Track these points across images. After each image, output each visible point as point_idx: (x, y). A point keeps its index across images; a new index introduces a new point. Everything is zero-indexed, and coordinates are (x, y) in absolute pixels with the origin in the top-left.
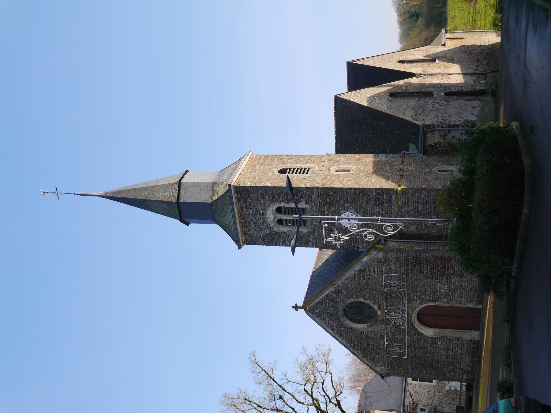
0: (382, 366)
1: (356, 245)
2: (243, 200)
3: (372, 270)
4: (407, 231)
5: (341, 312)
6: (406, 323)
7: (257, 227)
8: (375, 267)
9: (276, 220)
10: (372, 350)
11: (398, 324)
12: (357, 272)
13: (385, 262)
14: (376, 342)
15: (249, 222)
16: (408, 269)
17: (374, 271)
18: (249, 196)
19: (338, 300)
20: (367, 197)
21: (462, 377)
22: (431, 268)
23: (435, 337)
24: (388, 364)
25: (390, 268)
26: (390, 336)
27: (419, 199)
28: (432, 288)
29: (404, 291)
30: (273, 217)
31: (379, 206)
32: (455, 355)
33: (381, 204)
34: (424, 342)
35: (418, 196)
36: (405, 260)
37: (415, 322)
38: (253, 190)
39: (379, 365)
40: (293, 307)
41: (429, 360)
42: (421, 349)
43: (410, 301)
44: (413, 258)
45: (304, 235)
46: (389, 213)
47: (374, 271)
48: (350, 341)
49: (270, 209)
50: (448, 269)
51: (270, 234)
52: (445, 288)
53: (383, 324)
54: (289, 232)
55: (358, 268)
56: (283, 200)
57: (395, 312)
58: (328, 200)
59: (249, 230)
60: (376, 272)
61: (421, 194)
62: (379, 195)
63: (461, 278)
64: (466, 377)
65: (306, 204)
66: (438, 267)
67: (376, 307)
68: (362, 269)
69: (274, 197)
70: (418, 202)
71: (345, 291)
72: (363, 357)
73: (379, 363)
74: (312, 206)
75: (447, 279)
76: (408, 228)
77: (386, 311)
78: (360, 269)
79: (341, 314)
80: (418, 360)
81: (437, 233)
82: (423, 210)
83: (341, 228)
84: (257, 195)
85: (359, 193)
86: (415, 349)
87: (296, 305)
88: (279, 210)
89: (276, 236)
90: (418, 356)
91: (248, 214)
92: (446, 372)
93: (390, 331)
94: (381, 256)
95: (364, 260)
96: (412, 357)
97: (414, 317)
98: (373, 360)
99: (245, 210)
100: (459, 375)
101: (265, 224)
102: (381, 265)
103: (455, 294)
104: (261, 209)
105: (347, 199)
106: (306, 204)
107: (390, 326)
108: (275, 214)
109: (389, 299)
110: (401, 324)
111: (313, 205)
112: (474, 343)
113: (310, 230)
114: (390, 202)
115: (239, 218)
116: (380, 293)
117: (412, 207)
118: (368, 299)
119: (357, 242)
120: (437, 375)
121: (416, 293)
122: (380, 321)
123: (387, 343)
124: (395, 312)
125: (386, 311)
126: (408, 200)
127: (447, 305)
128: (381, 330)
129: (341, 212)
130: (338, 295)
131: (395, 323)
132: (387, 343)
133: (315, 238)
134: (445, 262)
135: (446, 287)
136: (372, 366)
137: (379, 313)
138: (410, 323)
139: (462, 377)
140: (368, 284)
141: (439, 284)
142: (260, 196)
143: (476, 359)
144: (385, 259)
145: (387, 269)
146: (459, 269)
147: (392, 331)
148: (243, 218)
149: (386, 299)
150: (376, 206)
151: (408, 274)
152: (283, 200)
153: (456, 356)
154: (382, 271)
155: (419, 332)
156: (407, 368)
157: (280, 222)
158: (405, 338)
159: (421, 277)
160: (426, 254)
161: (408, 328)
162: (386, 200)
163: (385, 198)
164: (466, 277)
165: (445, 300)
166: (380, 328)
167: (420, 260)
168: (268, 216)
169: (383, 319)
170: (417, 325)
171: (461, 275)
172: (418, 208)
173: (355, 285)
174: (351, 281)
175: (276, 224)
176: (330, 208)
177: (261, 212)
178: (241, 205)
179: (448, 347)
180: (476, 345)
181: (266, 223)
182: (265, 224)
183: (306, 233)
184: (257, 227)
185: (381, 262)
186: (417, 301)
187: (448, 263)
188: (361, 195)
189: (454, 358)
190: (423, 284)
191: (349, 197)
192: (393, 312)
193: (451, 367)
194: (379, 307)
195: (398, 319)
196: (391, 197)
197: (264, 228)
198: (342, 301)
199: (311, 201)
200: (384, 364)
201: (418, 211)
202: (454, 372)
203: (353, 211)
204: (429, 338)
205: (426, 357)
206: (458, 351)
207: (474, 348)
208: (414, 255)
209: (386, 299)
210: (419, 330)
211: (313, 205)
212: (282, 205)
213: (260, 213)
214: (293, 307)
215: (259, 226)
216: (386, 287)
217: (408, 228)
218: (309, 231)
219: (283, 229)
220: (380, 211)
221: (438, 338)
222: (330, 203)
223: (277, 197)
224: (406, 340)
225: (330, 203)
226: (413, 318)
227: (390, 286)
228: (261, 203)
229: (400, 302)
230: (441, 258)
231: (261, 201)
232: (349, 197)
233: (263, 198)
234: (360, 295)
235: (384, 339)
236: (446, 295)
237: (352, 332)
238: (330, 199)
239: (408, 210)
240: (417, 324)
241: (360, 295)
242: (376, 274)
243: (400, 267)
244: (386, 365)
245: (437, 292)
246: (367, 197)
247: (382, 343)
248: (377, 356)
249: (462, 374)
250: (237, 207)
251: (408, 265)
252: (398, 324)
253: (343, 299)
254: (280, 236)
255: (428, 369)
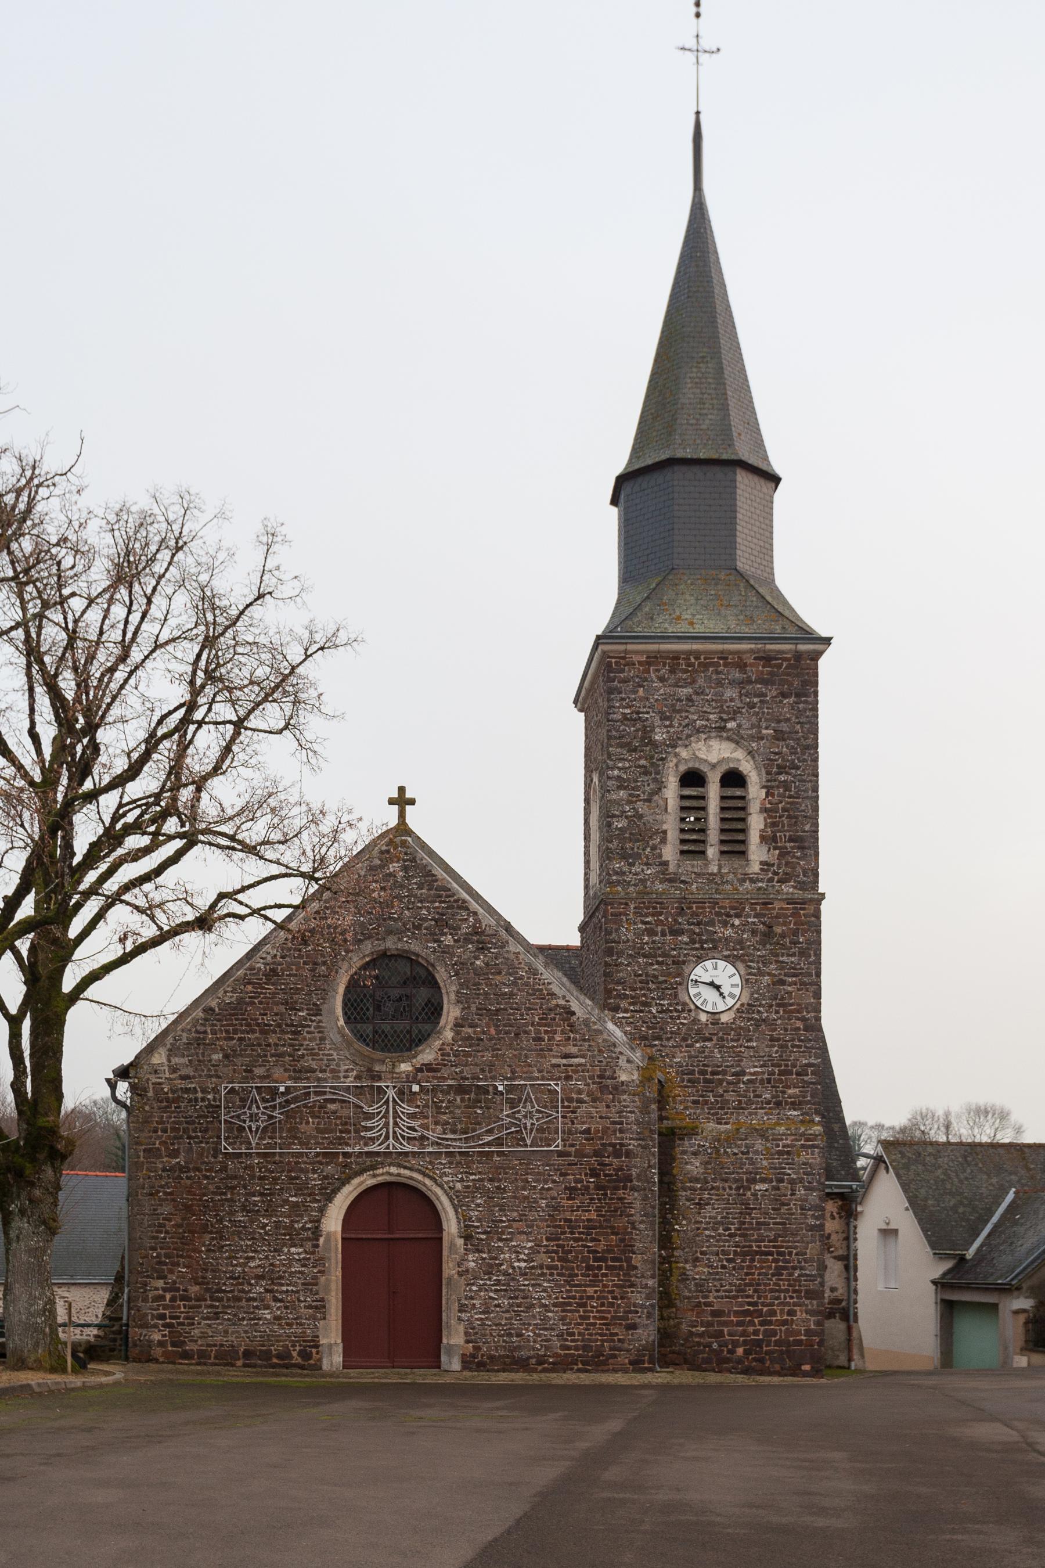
0: (174, 1070)
1: (624, 1004)
2: (770, 673)
3: (574, 1050)
4: (684, 1152)
5: (400, 946)
6: (373, 1148)
7: (673, 705)
8: (583, 1056)
9: (705, 768)
10: (240, 1039)
11: (369, 1124)
12: (562, 1002)
13: (603, 1089)
14: (281, 1055)
15: (694, 681)
16: (580, 1154)
17: (566, 1056)
18: (784, 695)
19: (448, 940)
20: (793, 1040)
21: (155, 1326)
22: (588, 1220)
23: (322, 1240)
24: (187, 1090)
25: (581, 1101)
26: (313, 1098)
27: (792, 1182)
28: (515, 1225)
29: (499, 1142)
30: (713, 758)
31: (763, 1073)
32: (254, 1299)
33: (769, 1081)
34: (296, 1205)
35: (801, 1181)
36: (614, 1145)
37: (374, 1176)
38: (805, 710)
39: (176, 1060)
40: (402, 790)
41: (220, 1221)
42: (261, 1194)
43: (462, 1160)
44: (621, 1169)
45: (654, 848)
46: (740, 1102)
47: (566, 1056)
48: (273, 970)
49: (740, 754)
50: (589, 1268)
51: (653, 744)
52: (519, 1261)
53: (358, 1078)
54: (661, 802)
55: (575, 1006)
56: (773, 795)
57: (412, 1116)
58: (778, 930)
59: (662, 679)
60: (564, 1061)
61: (806, 1189)
62: (798, 1074)
63: (555, 1305)
64: (156, 1337)
65: (762, 863)
66: (593, 1240)
67: (427, 1055)
68: (574, 1018)
69: (781, 770)
70: (782, 1181)
71: (487, 964)
72: (209, 1010)
73: (185, 1060)
74: (752, 881)
75: (549, 1267)
76: (695, 1154)
77: (416, 1088)
78: (574, 1013)
79: (391, 944)
80: (211, 1188)
81: (682, 1235)
82: (755, 1195)
83: (684, 962)
84: (788, 720)
85: (803, 1019)
86: (261, 1178)
87: (412, 802)
88: (733, 779)
89: (643, 762)
90: (234, 1188)
91: (720, 683)
92: (172, 1277)
93: (333, 1101)
94: (624, 1077)
95: (610, 1026)
96: (224, 1169)
97: (393, 1172)
98: (199, 1042)
99: (737, 675)
100: (162, 1317)
101: (686, 731)
102: (591, 1078)
103: (496, 1291)
104: (739, 726)
105: (783, 983)
106: (762, 863)
107: (352, 1099)
108: (723, 768)
109: (462, 1100)
110: (369, 1134)
111: (760, 884)
112: (305, 1355)
113: (672, 868)
114: (778, 1104)
115: (705, 652)
116: (483, 1071)
117: (765, 1163)
118: (458, 1033)
119: (637, 1008)
120: (153, 1249)
121: (491, 1180)
122: (370, 1070)
123: (282, 1089)
124: (412, 1116)
125: (416, 1088)
126: (788, 1153)
127: (449, 1269)
128: (333, 1071)
129: (741, 966)
130: (467, 940)
131: (369, 1117)
132: (282, 1089)
133: (643, 881)
134: (614, 1260)
135: (523, 1265)
136: (170, 1040)
137: (405, 1067)
138: (372, 1161)
139: (155, 1326)
140: (517, 1035)
141: (530, 1244)
142: (784, 727)
143: (239, 1363)
144: (616, 1088)
145: (580, 1092)
146: (591, 1298)
147: (332, 1107)
148: (705, 666)
149: (461, 1090)
150: (761, 1066)
151: (560, 1154)
152: (773, 795)
153: (244, 1303)
154: (568, 1078)
155: (336, 1191)
156: (175, 1154)
157: (693, 778)
158: (302, 1144)
159: (554, 1193)
160: (638, 1205)
161: (346, 1155)
162: (784, 1092)
163: (790, 1091)
164: (563, 1319)
165: (472, 1264)
166: (343, 1068)
167: (616, 1188)
168: (715, 744)
169: (380, 1079)
170: (360, 1184)
171: (570, 1304)
172: (763, 1180)
173: (512, 995)
174: (527, 984)
175: (690, 765)
176: (754, 932)
177: (731, 725)
178: (751, 665)
179: (281, 1278)
180: (296, 1359)
181: (689, 736)
182: (686, 731)
183: (660, 856)
184: (673, 705)
185: (601, 1077)
186: (462, 1180)
187: (608, 1268)
188: (799, 1024)
189: (239, 1299)
190: (526, 1198)
191: (790, 989)
192: (412, 1110)
193: (194, 1289)
194: (429, 1067)
195: (387, 1124)
196: (794, 1106)
197: (671, 726)
198: (446, 951)
199: (771, 880)
200: (183, 1078)
201: (754, 1181)
202: (173, 1299)
203: (745, 1000)
204: (319, 1221)
205: (232, 1213)
206: (267, 1307)
207: (284, 1355)
208: (634, 1172)
209: (461, 1090)
210: (346, 1189)
211: (760, 884)
212: (755, 791)
213: (726, 721)
214: (402, 790)
215: (679, 711)
216: (510, 1089)
217: (695, 1154)
218: (666, 864)
219: (672, 791)
220: (745, 1078)
221: (317, 1246)
222: (768, 934)
223: (782, 778)
224: (296, 1149)
225: (768, 934)
226: (394, 1170)
227: (513, 1104)
228: (759, 727)
229: (454, 1132)
230: (628, 1248)
231: (767, 728)
232: (790, 989)
233: (779, 736)
234: (473, 1008)
235: (296, 1079)
236: (491, 1266)
237: (316, 977)
238: (783, 936)
239: (756, 1152)
240: (367, 1181)
241: (473, 1008)
242: (554, 1061)
243: (587, 1131)
244: (180, 1084)
245: (500, 1240)
246: (793, 1040)
247: (278, 1072)
248: (217, 1057)
249: (165, 1326)
250: (752, 651)
251: (596, 1153)
252: (369, 1124)
253: (453, 955)
254: (646, 773)
255: (178, 1219)
